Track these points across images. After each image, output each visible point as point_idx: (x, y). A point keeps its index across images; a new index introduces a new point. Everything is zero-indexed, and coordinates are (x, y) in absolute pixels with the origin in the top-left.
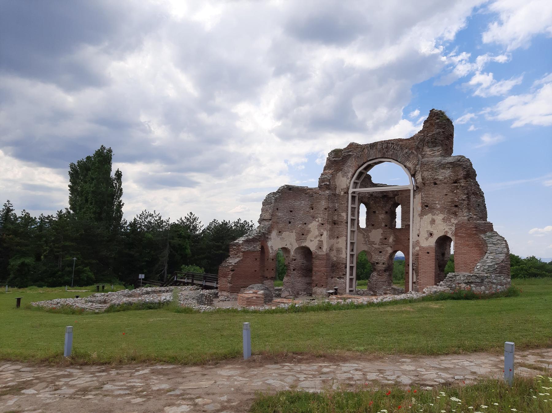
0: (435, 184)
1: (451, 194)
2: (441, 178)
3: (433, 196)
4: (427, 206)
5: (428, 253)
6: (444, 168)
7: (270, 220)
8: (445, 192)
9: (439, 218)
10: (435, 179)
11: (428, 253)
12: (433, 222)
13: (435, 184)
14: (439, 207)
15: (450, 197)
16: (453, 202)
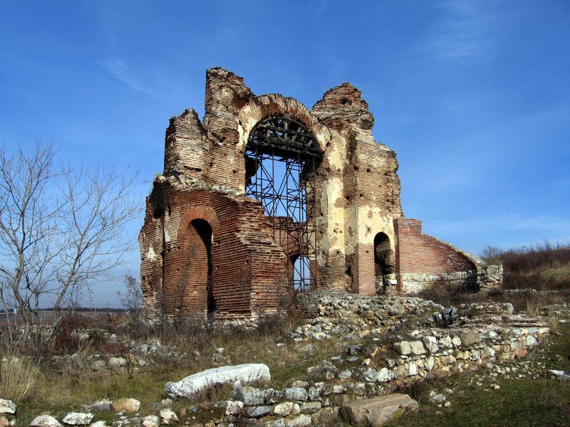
0: (368, 170)
1: (384, 186)
2: (375, 165)
3: (368, 185)
4: (361, 195)
5: (367, 252)
6: (380, 156)
7: (199, 170)
8: (379, 183)
9: (376, 210)
10: (370, 166)
11: (367, 252)
12: (370, 215)
13: (368, 170)
14: (375, 198)
15: (383, 190)
16: (386, 195)
